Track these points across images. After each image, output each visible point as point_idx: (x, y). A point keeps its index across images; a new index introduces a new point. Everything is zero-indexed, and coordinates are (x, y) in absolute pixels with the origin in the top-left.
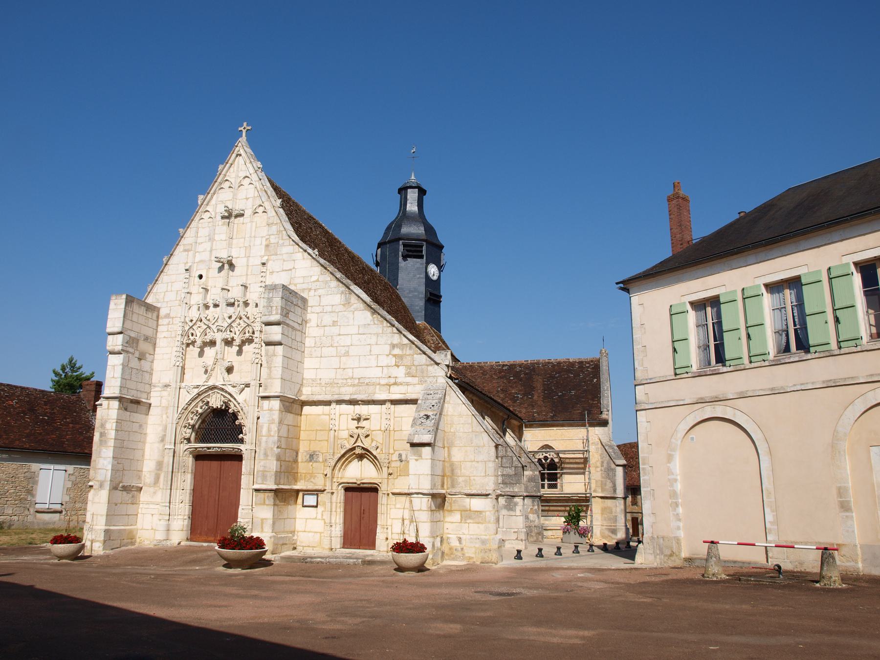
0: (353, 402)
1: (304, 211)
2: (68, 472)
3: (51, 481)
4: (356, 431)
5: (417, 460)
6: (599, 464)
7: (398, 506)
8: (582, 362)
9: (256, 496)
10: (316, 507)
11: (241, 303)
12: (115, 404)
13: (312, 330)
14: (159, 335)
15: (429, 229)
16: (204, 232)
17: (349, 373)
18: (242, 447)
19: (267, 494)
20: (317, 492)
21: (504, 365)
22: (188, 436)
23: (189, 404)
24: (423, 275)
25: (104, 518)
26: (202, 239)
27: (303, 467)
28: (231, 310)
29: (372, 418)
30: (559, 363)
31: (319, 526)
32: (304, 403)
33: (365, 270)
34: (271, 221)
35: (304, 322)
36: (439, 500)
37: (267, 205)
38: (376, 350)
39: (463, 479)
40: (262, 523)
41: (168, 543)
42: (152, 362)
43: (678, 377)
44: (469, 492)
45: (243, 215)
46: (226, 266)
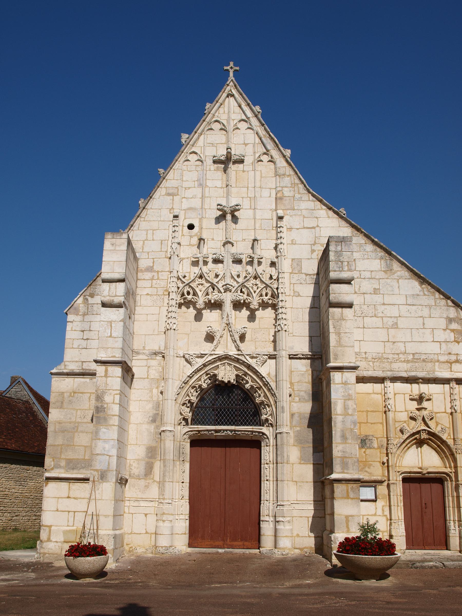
17: (401, 347)
18: (264, 430)
19: (350, 486)
20: (374, 484)
28: (237, 268)
29: (434, 397)
37: (274, 153)
38: (430, 323)
40: (347, 521)
46: (229, 217)
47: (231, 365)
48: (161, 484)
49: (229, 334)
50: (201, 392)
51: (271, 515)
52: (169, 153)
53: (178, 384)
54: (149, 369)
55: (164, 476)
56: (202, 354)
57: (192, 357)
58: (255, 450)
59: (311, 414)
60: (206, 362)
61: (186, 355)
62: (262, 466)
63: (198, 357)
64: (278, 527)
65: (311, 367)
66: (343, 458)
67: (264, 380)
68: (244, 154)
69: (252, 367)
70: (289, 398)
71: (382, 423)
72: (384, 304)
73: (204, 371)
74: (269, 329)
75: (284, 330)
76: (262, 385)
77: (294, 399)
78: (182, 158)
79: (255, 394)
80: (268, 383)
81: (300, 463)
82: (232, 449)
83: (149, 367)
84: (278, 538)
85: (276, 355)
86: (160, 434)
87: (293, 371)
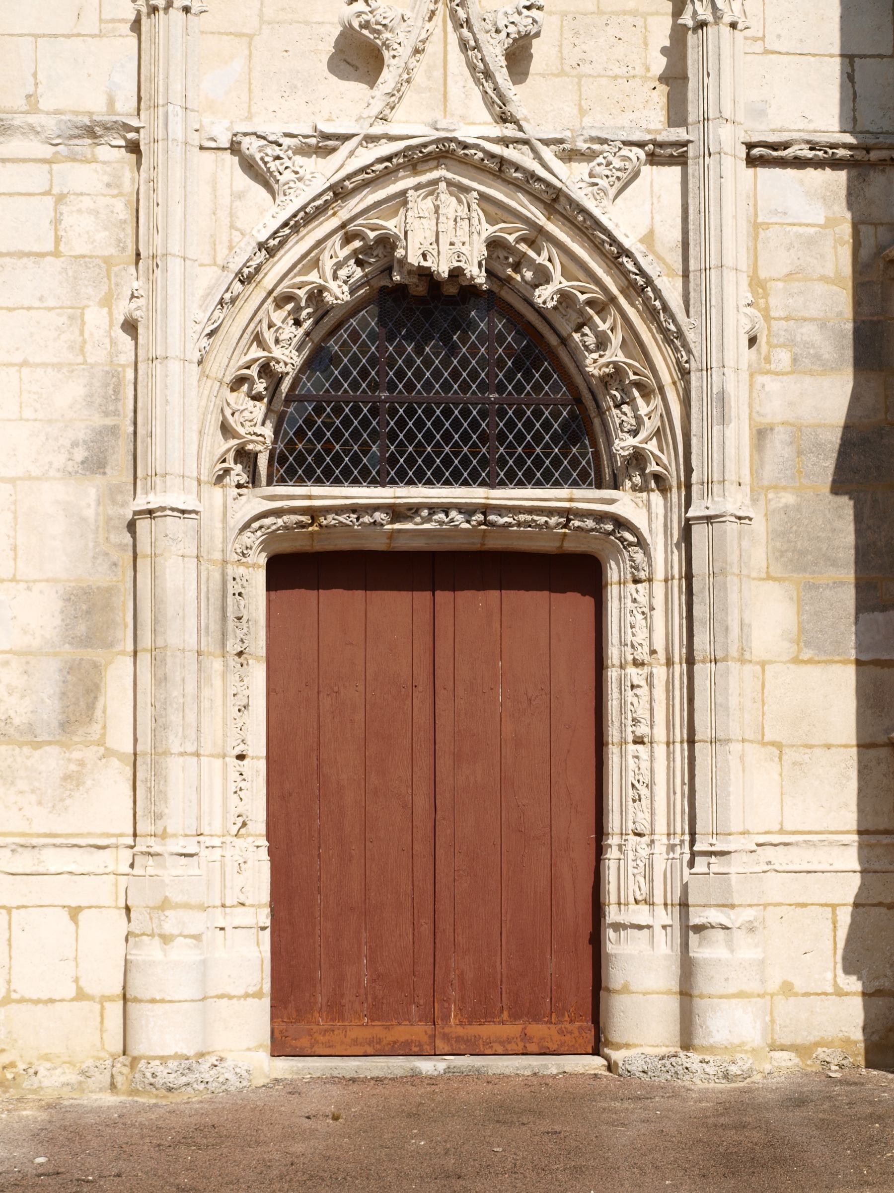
18: (625, 503)
47: (466, 190)
48: (143, 769)
49: (453, 38)
50: (316, 323)
51: (659, 899)
53: (211, 281)
54: (63, 208)
55: (160, 725)
56: (327, 137)
57: (277, 151)
58: (573, 605)
59: (847, 428)
60: (349, 177)
61: (246, 142)
62: (612, 674)
63: (305, 151)
64: (700, 951)
65: (850, 206)
67: (630, 266)
69: (571, 201)
70: (747, 355)
73: (334, 222)
74: (645, 16)
75: (727, 19)
76: (615, 291)
77: (768, 360)
79: (577, 336)
80: (649, 282)
81: (796, 661)
82: (465, 596)
83: (61, 199)
84: (700, 1004)
85: (685, 144)
86: (131, 527)
87: (767, 226)
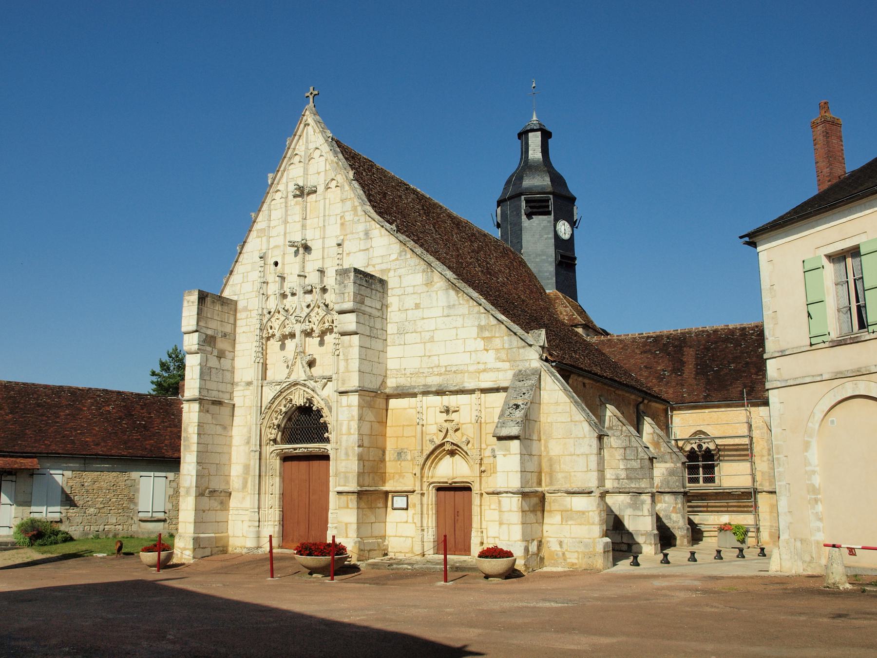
0: (440, 393)
1: (393, 177)
2: (169, 479)
3: (149, 488)
4: (446, 425)
5: (504, 455)
6: (765, 452)
7: (493, 507)
8: (744, 329)
9: (339, 499)
10: (407, 509)
11: (318, 290)
12: (196, 406)
13: (394, 315)
14: (238, 330)
15: (557, 180)
16: (277, 214)
18: (328, 447)
20: (406, 493)
21: (648, 337)
22: (273, 437)
23: (272, 402)
24: (552, 235)
25: (192, 526)
26: (276, 223)
27: (390, 466)
28: (309, 298)
30: (715, 331)
31: (411, 530)
32: (388, 397)
33: (475, 236)
34: (344, 197)
35: (384, 307)
36: (535, 500)
39: (563, 475)
40: (346, 528)
41: (260, 551)
42: (233, 360)
43: (814, 347)
44: (570, 489)
45: (315, 192)
46: (301, 250)
52: (256, 196)
66: (345, 473)
68: (315, 184)
71: (415, 437)
72: (423, 319)
78: (268, 200)
